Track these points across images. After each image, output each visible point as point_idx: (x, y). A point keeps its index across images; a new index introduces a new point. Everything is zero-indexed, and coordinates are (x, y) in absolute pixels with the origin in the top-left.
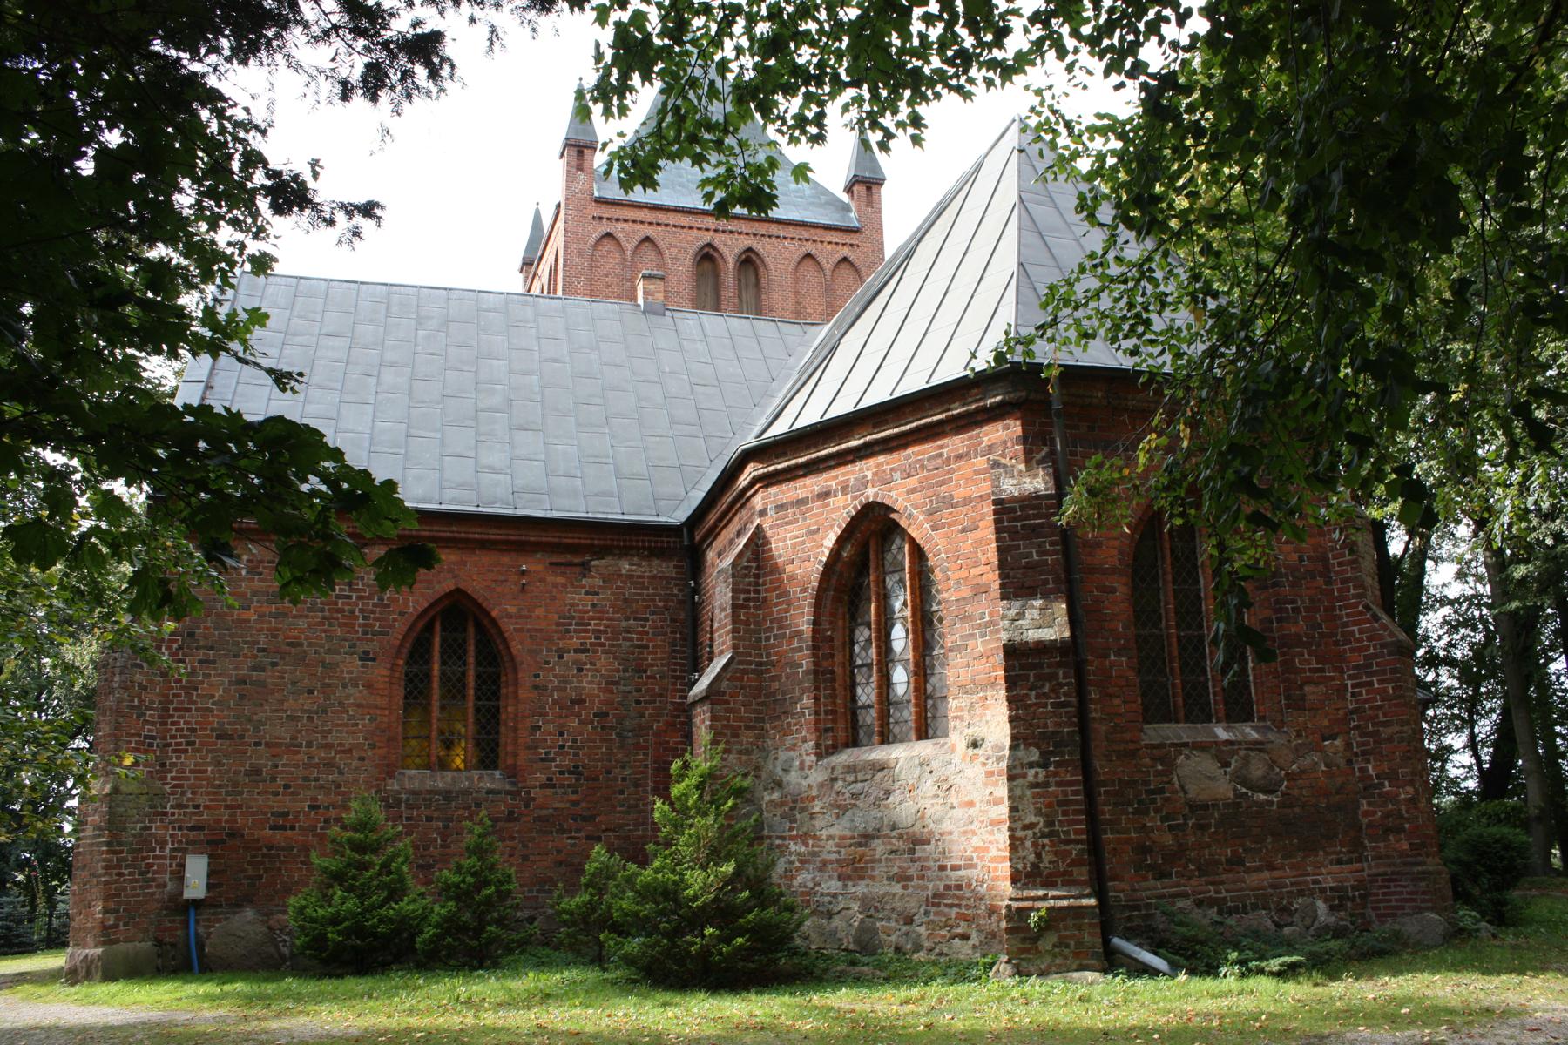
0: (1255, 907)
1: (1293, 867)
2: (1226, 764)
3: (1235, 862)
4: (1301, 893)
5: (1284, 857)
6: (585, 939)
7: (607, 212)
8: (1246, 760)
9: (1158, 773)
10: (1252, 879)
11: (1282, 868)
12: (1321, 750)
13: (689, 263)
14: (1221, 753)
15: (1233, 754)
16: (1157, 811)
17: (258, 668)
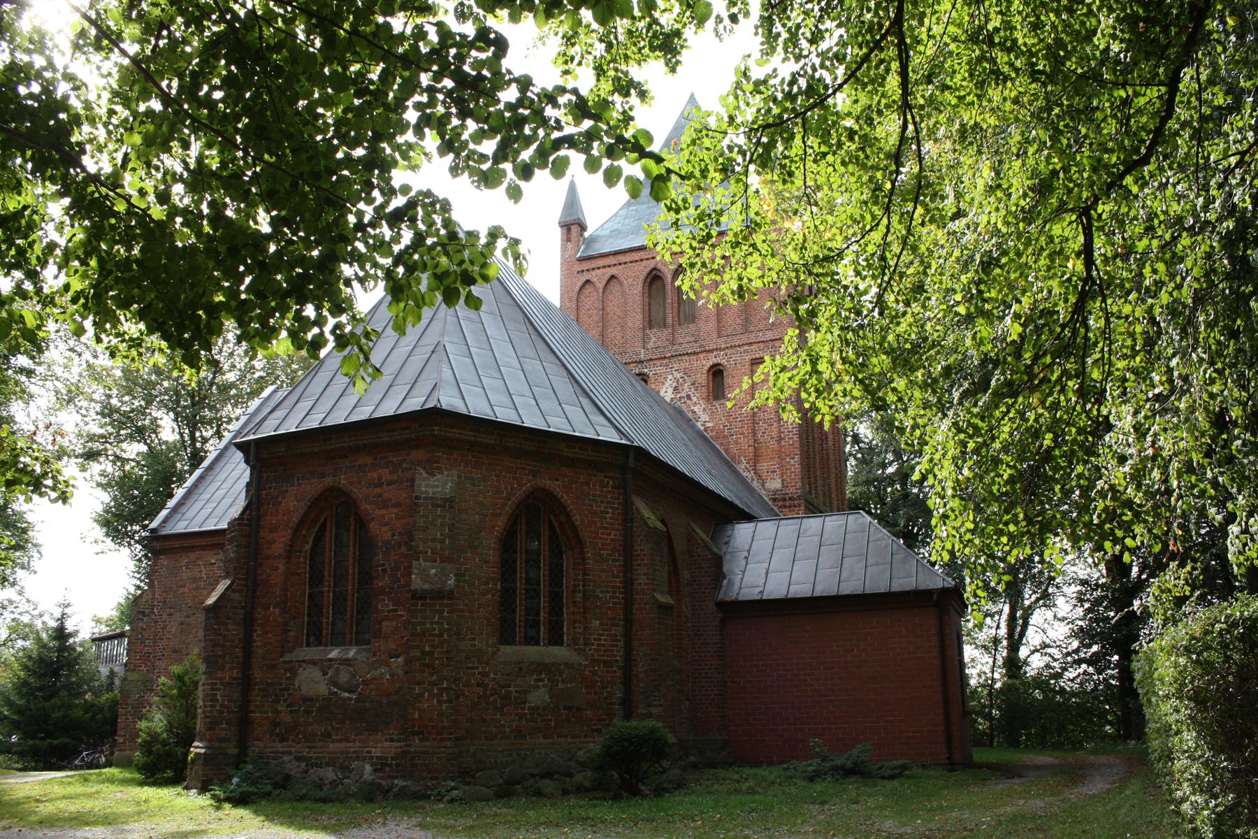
0: (327, 764)
1: (361, 741)
2: (325, 674)
3: (327, 736)
4: (358, 758)
5: (357, 735)
6: (321, 772)
7: (586, 266)
8: (338, 670)
9: (288, 679)
10: (332, 747)
11: (354, 741)
12: (387, 664)
13: (640, 287)
14: (325, 666)
15: (330, 667)
16: (285, 701)
17: (187, 617)
